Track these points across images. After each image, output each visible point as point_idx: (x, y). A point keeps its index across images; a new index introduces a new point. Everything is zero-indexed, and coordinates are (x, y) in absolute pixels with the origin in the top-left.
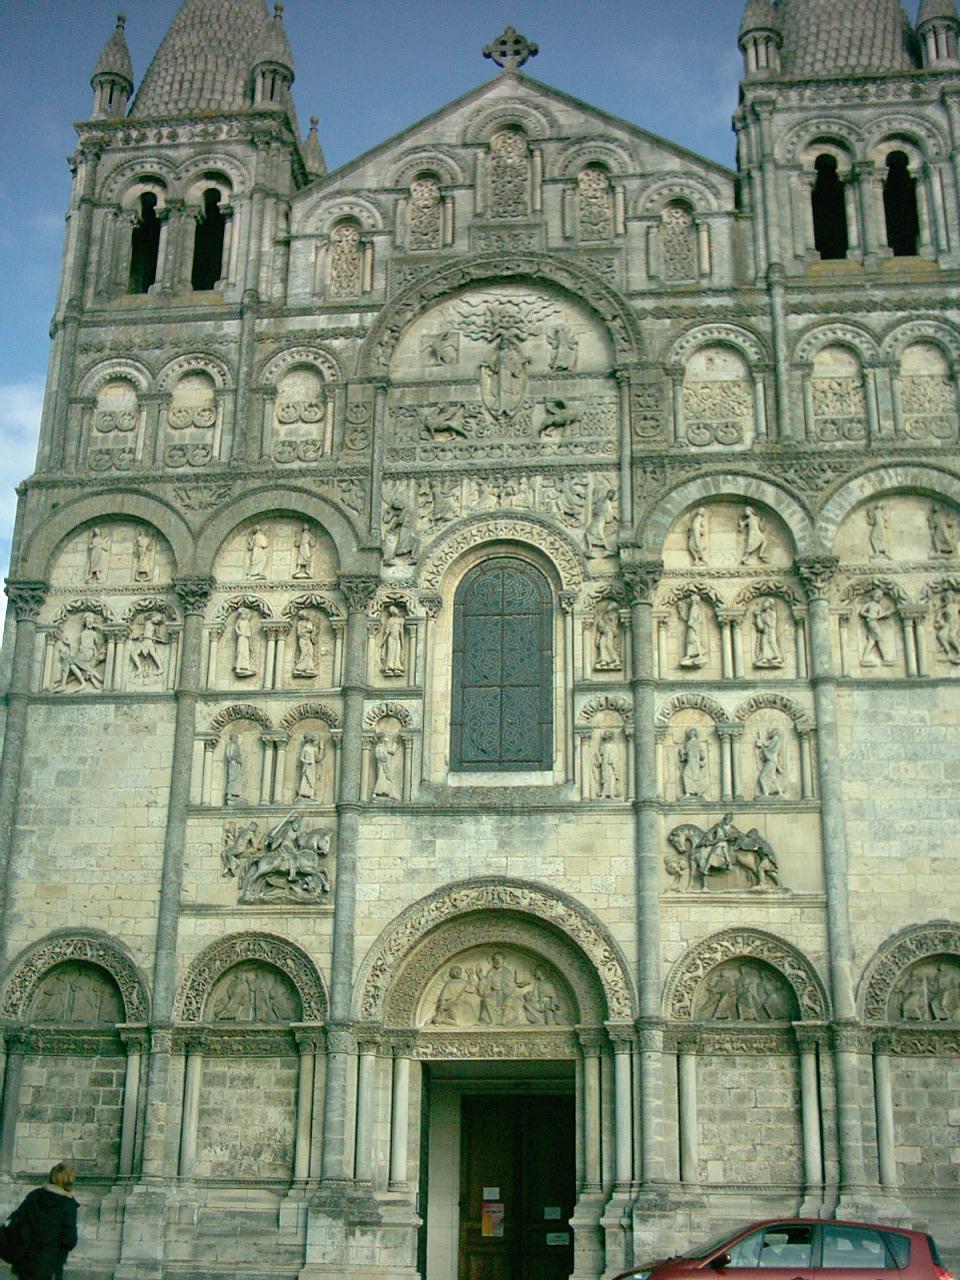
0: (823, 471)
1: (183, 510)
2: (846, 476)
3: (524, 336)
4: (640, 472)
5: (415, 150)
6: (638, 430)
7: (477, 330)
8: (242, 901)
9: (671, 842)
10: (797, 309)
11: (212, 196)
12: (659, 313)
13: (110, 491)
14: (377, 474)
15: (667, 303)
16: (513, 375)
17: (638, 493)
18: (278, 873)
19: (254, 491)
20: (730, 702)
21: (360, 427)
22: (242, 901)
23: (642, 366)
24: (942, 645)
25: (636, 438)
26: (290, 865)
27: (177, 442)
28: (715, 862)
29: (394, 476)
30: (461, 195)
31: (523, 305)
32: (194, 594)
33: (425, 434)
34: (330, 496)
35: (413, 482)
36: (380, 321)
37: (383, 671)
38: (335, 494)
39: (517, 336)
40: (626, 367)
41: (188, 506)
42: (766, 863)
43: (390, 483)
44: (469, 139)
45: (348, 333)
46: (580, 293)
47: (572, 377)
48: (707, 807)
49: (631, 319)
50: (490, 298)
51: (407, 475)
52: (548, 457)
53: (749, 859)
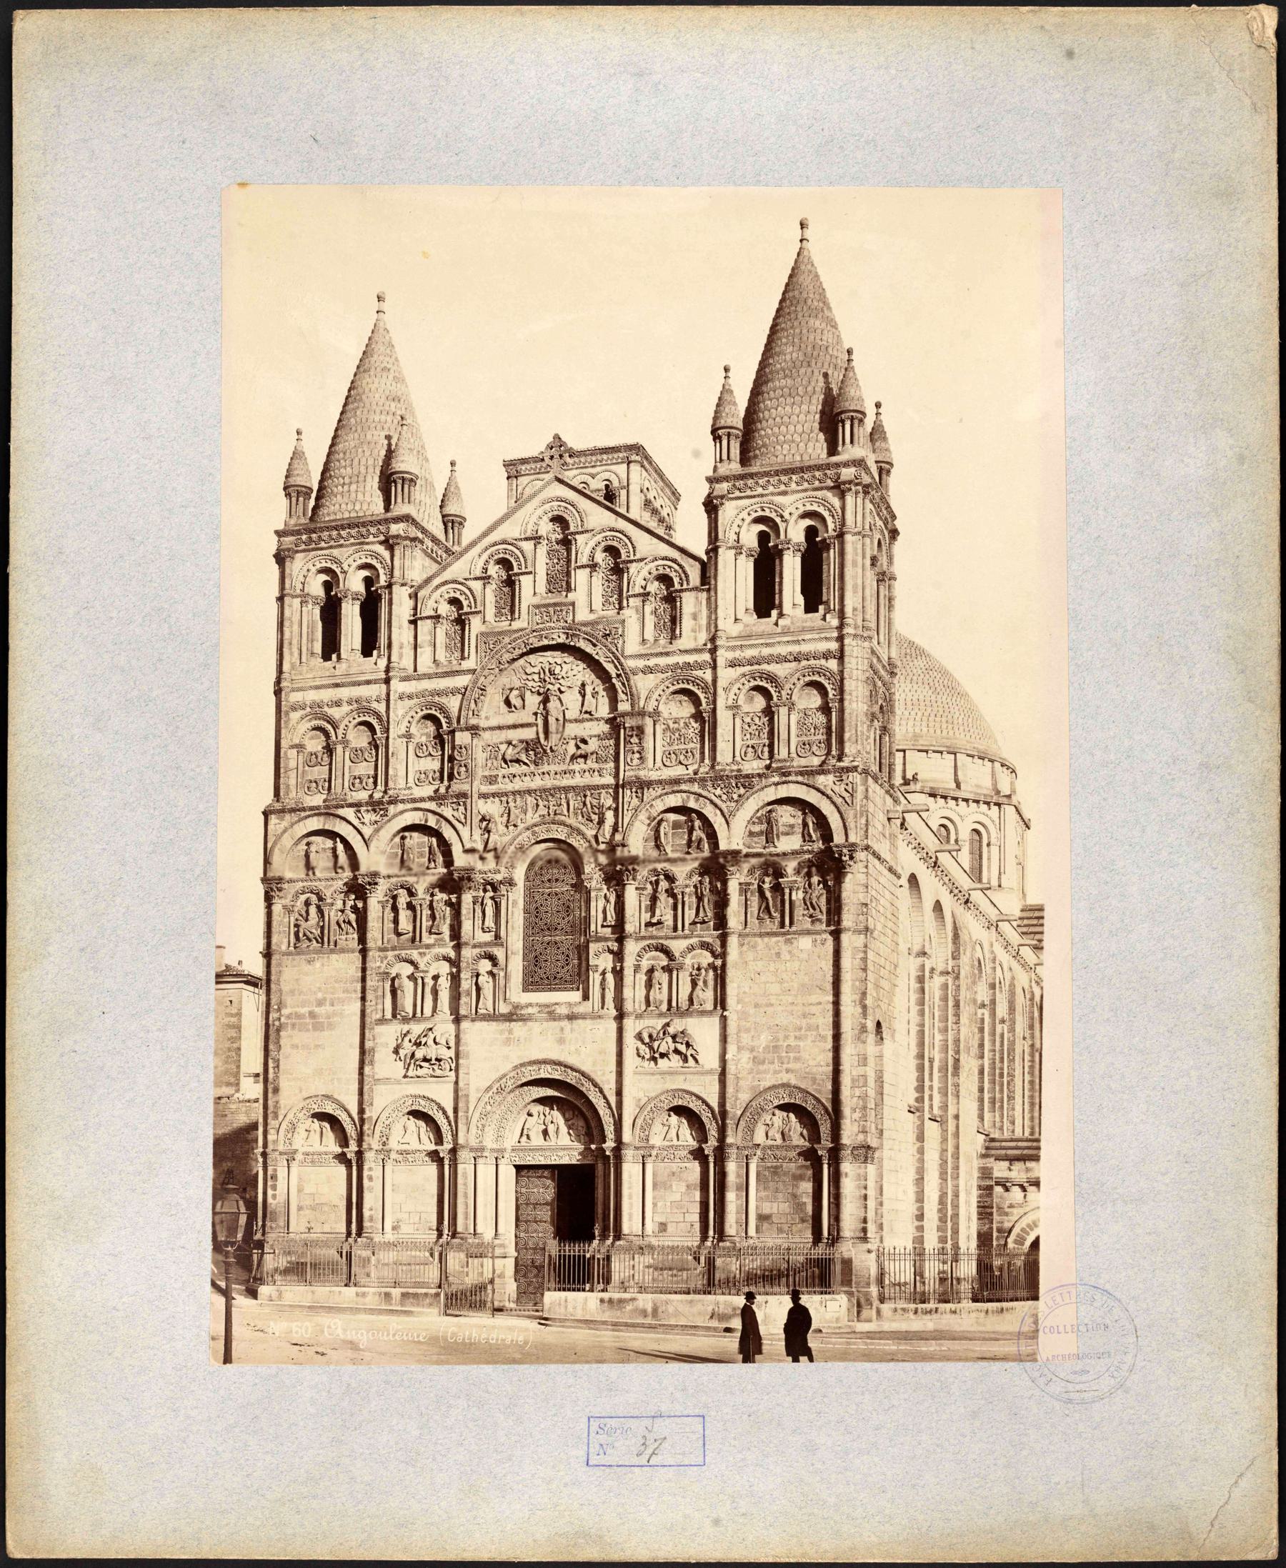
0: (738, 788)
1: (360, 826)
2: (751, 791)
3: (563, 689)
4: (629, 792)
5: (495, 544)
6: (629, 760)
7: (535, 685)
8: (405, 1076)
9: (639, 1037)
10: (733, 664)
11: (369, 582)
12: (648, 670)
13: (315, 815)
14: (475, 796)
15: (652, 662)
16: (557, 720)
17: (626, 807)
18: (425, 1060)
19: (402, 812)
20: (677, 946)
21: (463, 763)
22: (405, 1076)
23: (631, 714)
24: (806, 904)
25: (627, 767)
26: (432, 1054)
27: (357, 774)
28: (662, 1050)
29: (484, 796)
30: (526, 581)
31: (563, 665)
32: (370, 884)
33: (504, 765)
34: (445, 814)
35: (497, 799)
36: (475, 682)
37: (483, 929)
38: (447, 812)
39: (559, 689)
40: (623, 715)
41: (363, 823)
42: (690, 1051)
43: (483, 800)
44: (528, 534)
45: (454, 692)
46: (597, 657)
47: (591, 720)
48: (661, 1015)
49: (625, 675)
50: (541, 659)
51: (494, 795)
52: (577, 781)
53: (682, 1048)
